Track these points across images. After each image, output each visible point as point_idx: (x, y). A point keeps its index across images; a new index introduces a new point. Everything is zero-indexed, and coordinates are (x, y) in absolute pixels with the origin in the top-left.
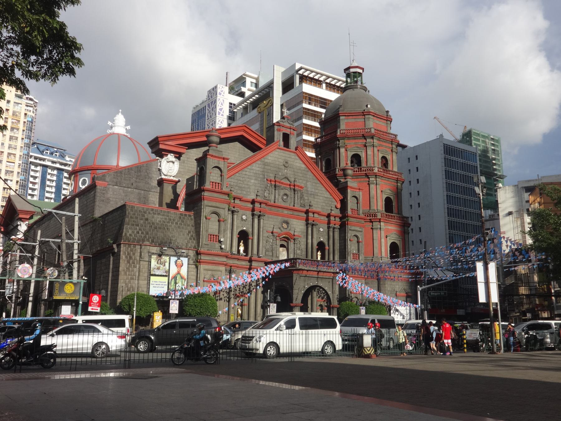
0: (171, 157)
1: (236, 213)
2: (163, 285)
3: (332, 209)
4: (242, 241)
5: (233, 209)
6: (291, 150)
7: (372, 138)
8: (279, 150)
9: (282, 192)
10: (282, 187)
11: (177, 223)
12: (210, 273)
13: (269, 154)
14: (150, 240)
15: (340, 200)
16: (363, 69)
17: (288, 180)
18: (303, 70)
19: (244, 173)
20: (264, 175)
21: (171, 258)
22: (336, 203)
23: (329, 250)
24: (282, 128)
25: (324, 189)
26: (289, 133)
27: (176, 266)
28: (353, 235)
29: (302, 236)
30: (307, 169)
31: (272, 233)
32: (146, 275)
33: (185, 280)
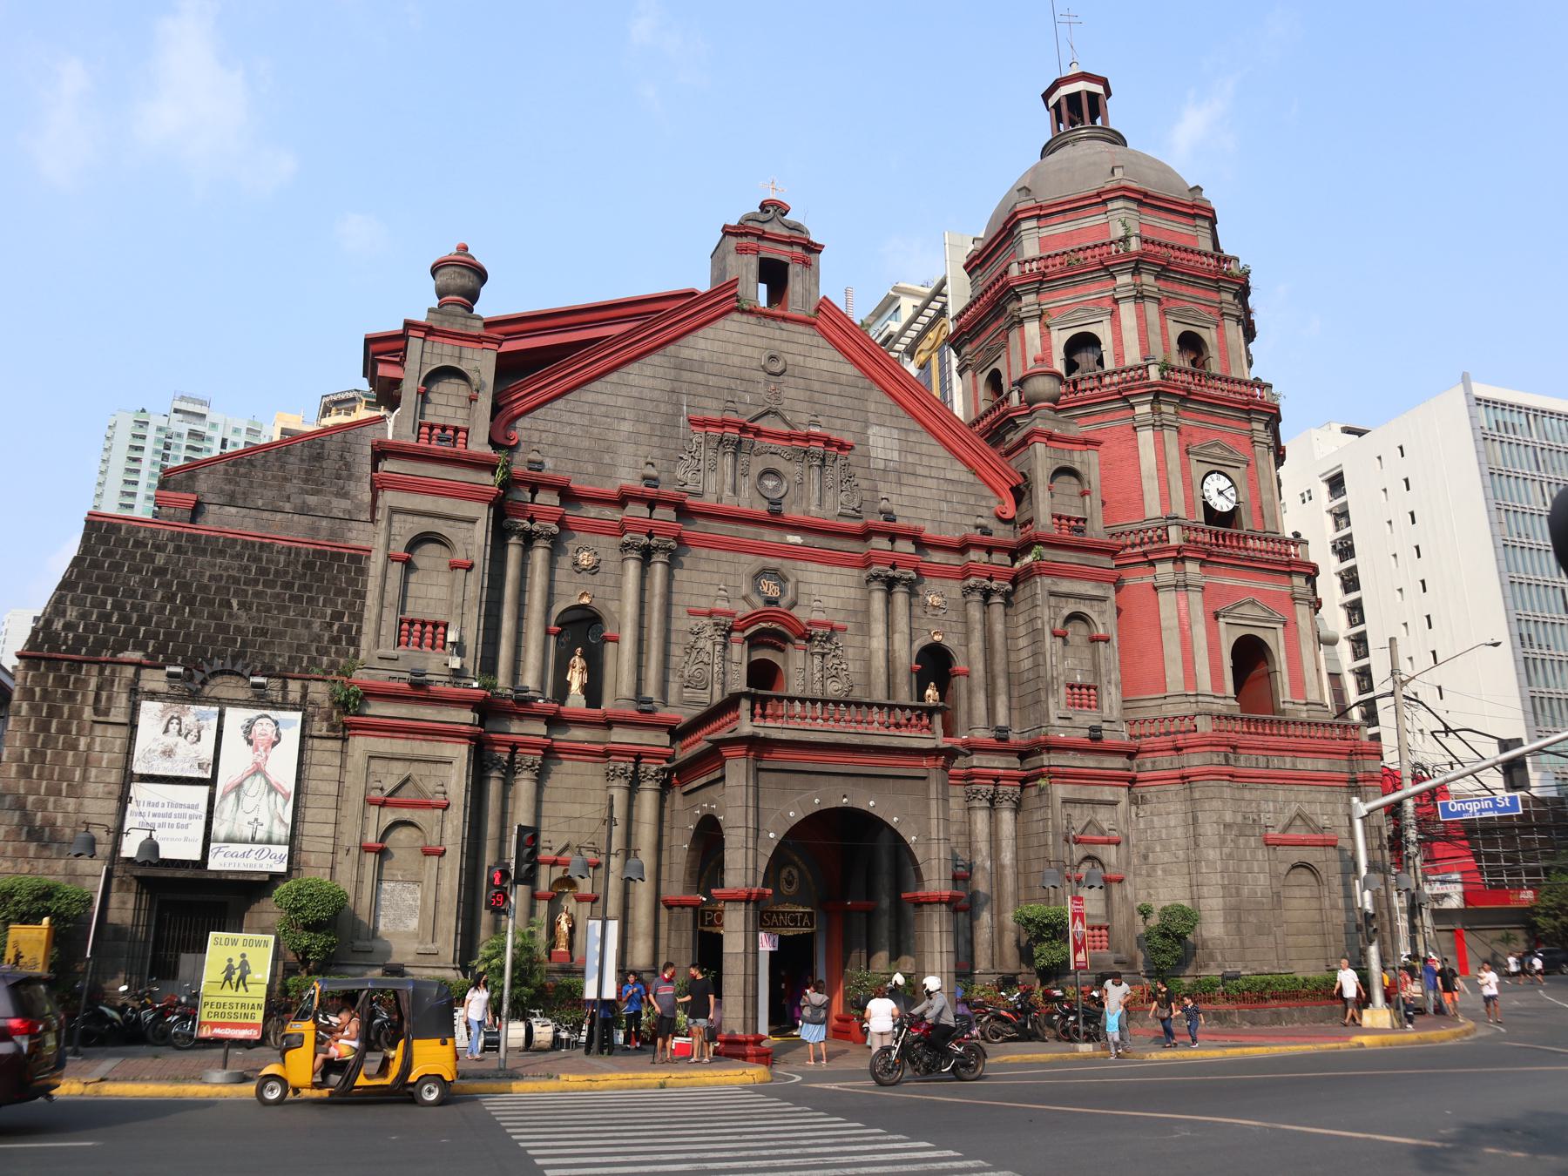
2: (183, 816)
9: (758, 465)
11: (288, 586)
12: (399, 770)
14: (151, 643)
15: (1012, 489)
16: (1104, 82)
20: (678, 404)
21: (229, 711)
25: (941, 451)
27: (250, 742)
28: (1066, 612)
30: (868, 382)
32: (114, 776)
33: (286, 797)
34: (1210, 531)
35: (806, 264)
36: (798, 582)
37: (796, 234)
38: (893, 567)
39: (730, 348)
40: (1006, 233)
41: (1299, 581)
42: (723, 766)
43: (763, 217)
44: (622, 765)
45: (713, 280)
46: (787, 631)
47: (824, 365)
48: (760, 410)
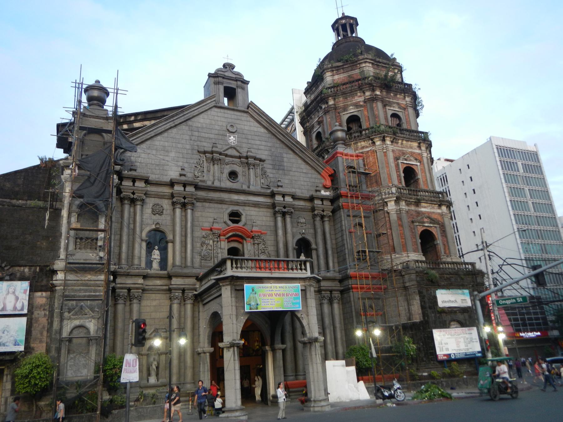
1: (139, 203)
3: (317, 189)
4: (156, 247)
5: (132, 196)
6: (240, 108)
7: (373, 91)
8: (219, 110)
10: (227, 161)
13: (201, 116)
15: (330, 176)
16: (355, 20)
17: (238, 151)
19: (157, 143)
22: (323, 181)
23: (316, 250)
24: (220, 79)
25: (300, 161)
29: (269, 233)
31: (211, 230)
34: (408, 190)
35: (243, 89)
36: (246, 215)
37: (238, 77)
38: (285, 207)
39: (213, 122)
40: (318, 78)
41: (444, 208)
42: (220, 290)
43: (224, 70)
44: (177, 294)
45: (205, 95)
46: (243, 235)
47: (252, 128)
48: (228, 147)
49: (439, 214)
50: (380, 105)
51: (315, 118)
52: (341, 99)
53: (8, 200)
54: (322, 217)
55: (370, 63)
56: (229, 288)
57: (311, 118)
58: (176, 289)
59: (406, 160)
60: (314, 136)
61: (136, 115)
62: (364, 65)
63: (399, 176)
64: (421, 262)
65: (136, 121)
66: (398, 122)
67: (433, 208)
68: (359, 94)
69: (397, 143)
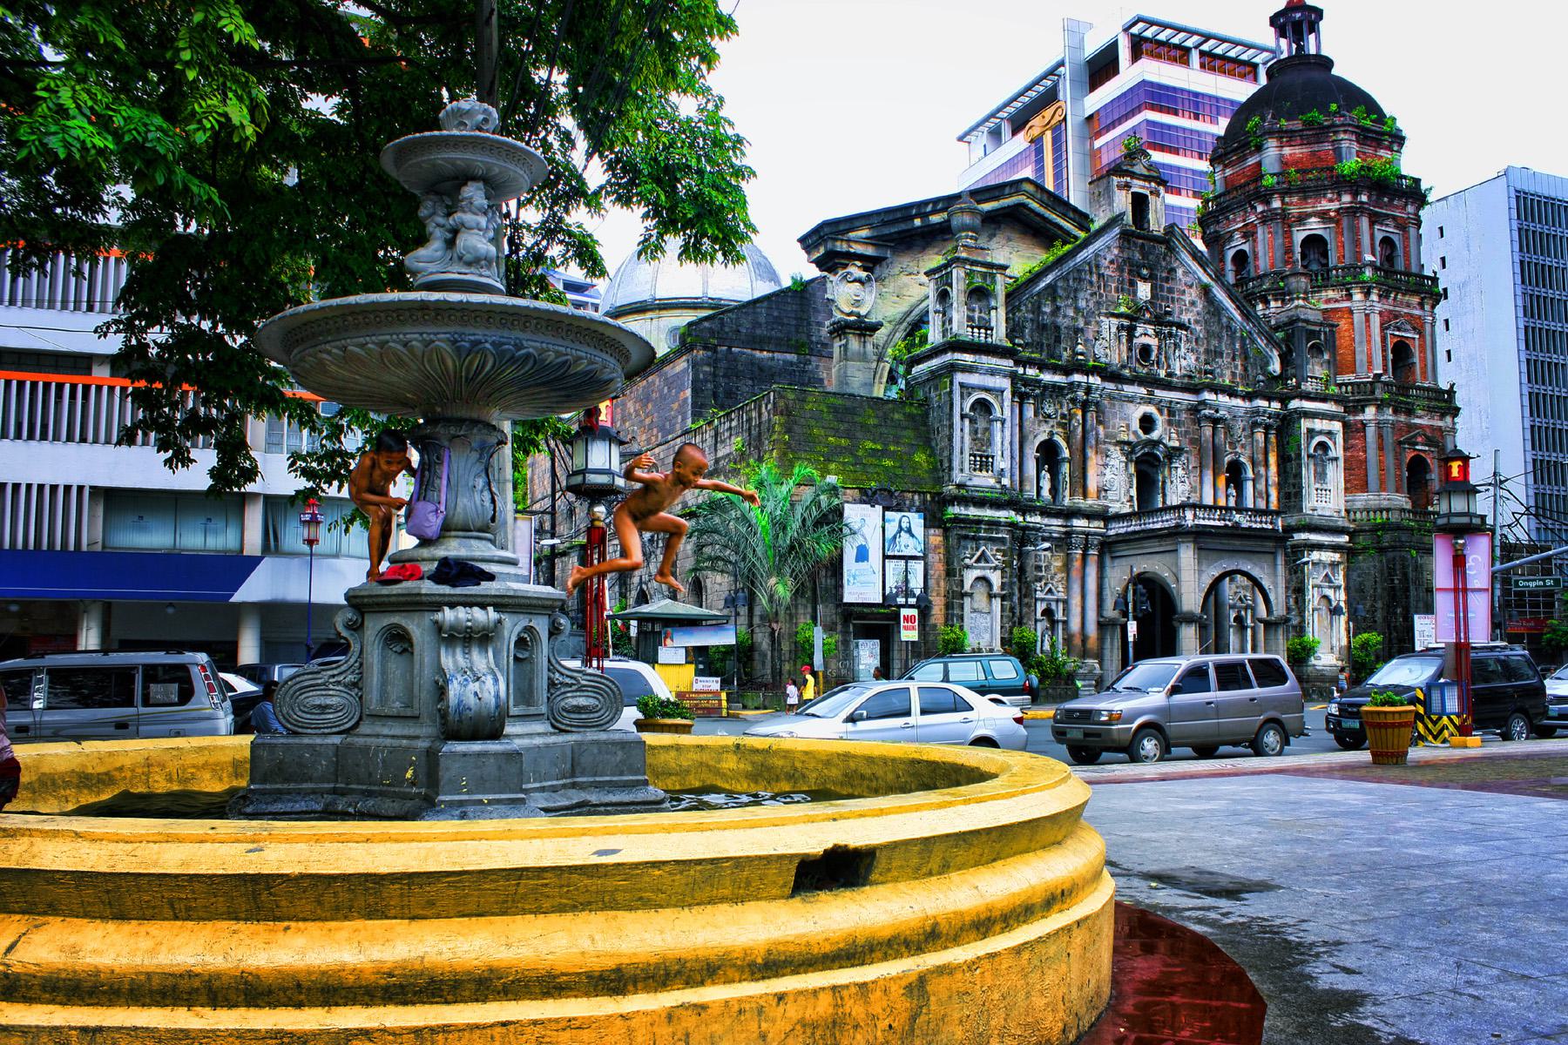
0: (856, 271)
7: (1355, 194)
18: (1141, 25)
26: (1148, 193)
49: (1440, 428)
50: (1364, 222)
51: (1234, 220)
52: (1295, 199)
53: (749, 351)
54: (1267, 428)
55: (1352, 132)
56: (1192, 545)
57: (1227, 218)
58: (1078, 533)
59: (1399, 330)
60: (1230, 254)
61: (935, 201)
62: (1342, 136)
63: (1385, 358)
64: (1403, 510)
65: (934, 212)
66: (1388, 252)
67: (1432, 418)
68: (1329, 196)
69: (1387, 297)
